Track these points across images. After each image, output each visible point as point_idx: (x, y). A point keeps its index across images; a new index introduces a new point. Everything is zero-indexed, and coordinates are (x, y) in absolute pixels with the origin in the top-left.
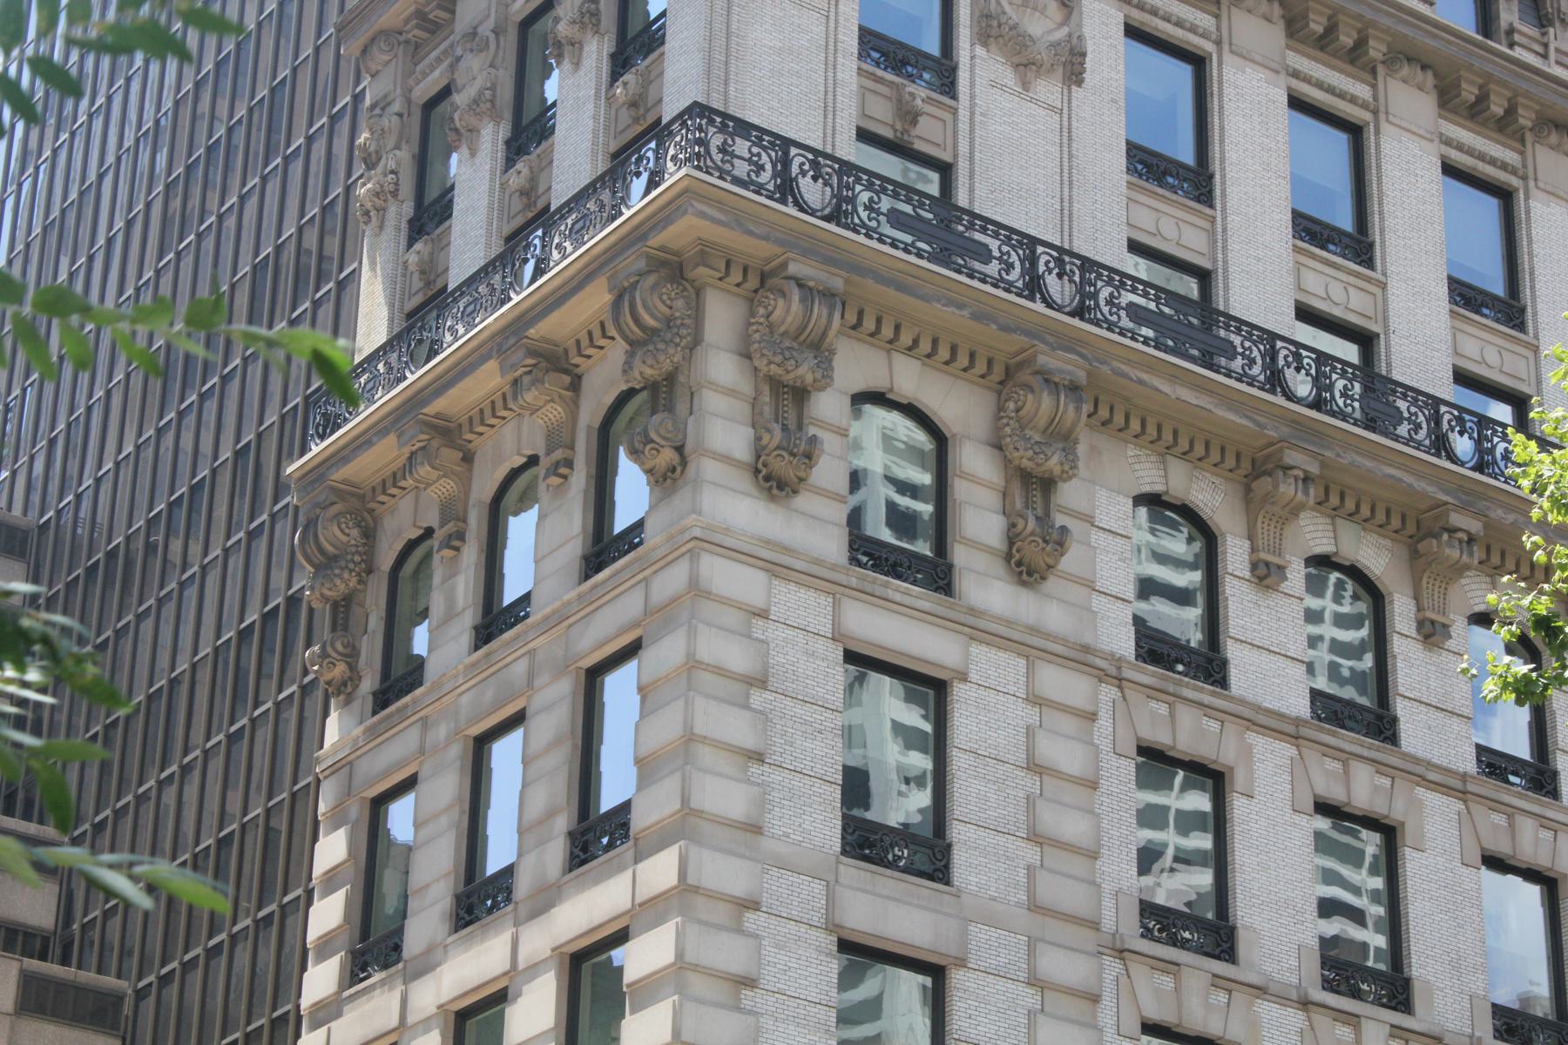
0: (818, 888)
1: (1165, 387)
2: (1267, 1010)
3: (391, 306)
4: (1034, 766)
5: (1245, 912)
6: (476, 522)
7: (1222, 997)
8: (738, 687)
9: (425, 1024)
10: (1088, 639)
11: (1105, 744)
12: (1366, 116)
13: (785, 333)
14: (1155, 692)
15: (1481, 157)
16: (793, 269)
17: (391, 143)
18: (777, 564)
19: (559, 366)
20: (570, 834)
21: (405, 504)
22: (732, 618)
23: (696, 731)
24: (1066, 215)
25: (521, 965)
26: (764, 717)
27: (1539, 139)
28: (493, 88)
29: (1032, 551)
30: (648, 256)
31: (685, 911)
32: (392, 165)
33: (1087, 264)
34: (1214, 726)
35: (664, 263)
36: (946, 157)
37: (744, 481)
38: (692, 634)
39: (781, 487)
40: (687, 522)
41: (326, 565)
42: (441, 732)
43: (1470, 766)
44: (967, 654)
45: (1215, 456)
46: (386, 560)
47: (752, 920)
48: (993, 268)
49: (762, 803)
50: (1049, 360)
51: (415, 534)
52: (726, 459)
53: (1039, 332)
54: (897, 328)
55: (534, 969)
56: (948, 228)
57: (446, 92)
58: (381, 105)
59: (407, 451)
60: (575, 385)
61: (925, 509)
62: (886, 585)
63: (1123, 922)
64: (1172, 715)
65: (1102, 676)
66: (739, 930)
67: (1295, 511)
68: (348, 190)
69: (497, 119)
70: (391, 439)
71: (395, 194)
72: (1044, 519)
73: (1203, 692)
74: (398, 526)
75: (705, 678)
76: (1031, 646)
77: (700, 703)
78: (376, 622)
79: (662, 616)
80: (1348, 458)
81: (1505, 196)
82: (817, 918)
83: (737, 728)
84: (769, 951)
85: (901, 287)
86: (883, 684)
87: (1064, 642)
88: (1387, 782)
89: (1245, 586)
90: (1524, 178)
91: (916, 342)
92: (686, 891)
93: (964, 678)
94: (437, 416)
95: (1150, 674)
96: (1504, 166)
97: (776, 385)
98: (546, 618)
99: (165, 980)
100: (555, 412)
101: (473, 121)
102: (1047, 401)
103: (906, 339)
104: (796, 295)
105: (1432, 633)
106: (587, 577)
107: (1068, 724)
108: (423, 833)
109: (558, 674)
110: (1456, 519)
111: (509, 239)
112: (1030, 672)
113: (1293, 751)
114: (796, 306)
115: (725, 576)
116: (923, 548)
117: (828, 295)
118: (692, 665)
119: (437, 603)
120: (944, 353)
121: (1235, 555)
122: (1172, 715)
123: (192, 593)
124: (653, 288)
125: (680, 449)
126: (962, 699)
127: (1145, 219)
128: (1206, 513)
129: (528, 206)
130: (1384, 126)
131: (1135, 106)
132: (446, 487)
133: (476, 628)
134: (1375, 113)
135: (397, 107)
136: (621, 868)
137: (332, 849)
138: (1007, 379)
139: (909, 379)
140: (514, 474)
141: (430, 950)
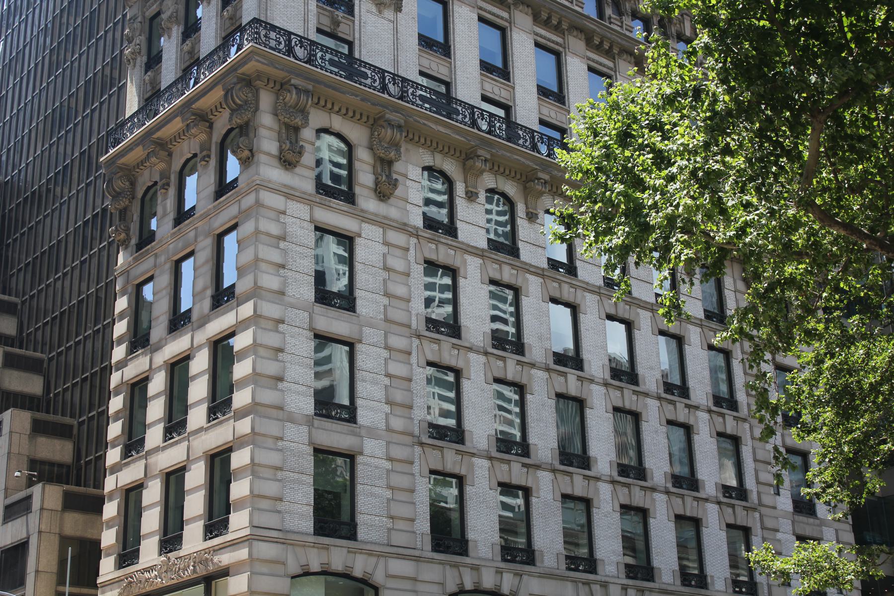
0: (306, 314)
1: (433, 126)
2: (472, 356)
3: (139, 96)
4: (386, 268)
5: (465, 320)
6: (174, 178)
7: (456, 352)
8: (274, 241)
9: (159, 369)
10: (405, 221)
11: (412, 260)
12: (507, 24)
13: (290, 107)
14: (430, 240)
15: (549, 40)
16: (293, 81)
17: (137, 34)
18: (289, 194)
19: (205, 119)
20: (213, 297)
21: (146, 173)
22: (272, 214)
23: (260, 256)
24: (396, 62)
25: (195, 346)
26: (285, 252)
27: (570, 34)
28: (177, 12)
29: (385, 188)
30: (238, 77)
31: (256, 324)
32: (138, 42)
33: (404, 80)
34: (453, 252)
35: (244, 80)
36: (351, 39)
37: (275, 162)
38: (257, 220)
39: (289, 165)
40: (255, 178)
41: (116, 196)
42: (162, 259)
43: (546, 266)
44: (361, 228)
45: (452, 152)
46: (140, 194)
47: (282, 327)
48: (369, 81)
49: (285, 283)
50: (390, 116)
51: (150, 184)
52: (269, 154)
53: (386, 105)
54: (333, 104)
55: (200, 347)
56: (352, 66)
57: (158, 14)
58: (134, 18)
59: (146, 152)
60: (211, 126)
61: (344, 173)
62: (330, 201)
63: (418, 324)
64: (437, 248)
65: (411, 235)
66: (277, 331)
67: (482, 172)
68: (122, 51)
69: (178, 24)
70: (140, 148)
71: (139, 53)
72: (389, 176)
73: (449, 240)
74: (145, 179)
75: (263, 237)
76: (384, 223)
77: (261, 247)
78: (136, 217)
79: (245, 214)
80: (501, 152)
81: (558, 55)
82: (306, 326)
83: (275, 256)
84: (288, 339)
85: (335, 89)
86: (330, 239)
87: (397, 222)
88: (515, 272)
89: (464, 201)
90: (565, 48)
91: (340, 109)
92: (257, 317)
93: (360, 236)
94: (158, 138)
95: (428, 233)
96: (557, 44)
97: (288, 126)
98: (202, 215)
99: (60, 354)
100: (203, 137)
101: (169, 25)
102: (389, 131)
103: (336, 108)
104: (294, 92)
105: (532, 217)
106: (217, 200)
107: (398, 252)
108: (156, 297)
109: (206, 237)
110: (541, 175)
111: (184, 70)
112: (384, 232)
113: (481, 261)
114: (294, 96)
115: (268, 198)
116: (344, 188)
117: (307, 92)
118: (257, 232)
119: (160, 210)
120: (351, 114)
121: (460, 189)
122: (437, 248)
123: (65, 207)
124: (240, 89)
125: (251, 151)
126: (359, 243)
127: (426, 63)
128: (449, 173)
129: (191, 58)
130: (513, 28)
131: (421, 19)
132: (162, 166)
133: (175, 219)
134: (510, 23)
135: (139, 19)
136: (232, 309)
137: (122, 304)
138: (374, 123)
139: (337, 123)
140: (188, 160)
141: (160, 340)
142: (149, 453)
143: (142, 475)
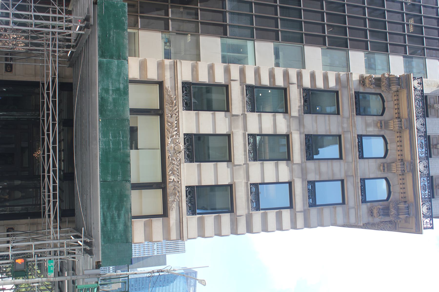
9: (289, 126)
143: (234, 113)
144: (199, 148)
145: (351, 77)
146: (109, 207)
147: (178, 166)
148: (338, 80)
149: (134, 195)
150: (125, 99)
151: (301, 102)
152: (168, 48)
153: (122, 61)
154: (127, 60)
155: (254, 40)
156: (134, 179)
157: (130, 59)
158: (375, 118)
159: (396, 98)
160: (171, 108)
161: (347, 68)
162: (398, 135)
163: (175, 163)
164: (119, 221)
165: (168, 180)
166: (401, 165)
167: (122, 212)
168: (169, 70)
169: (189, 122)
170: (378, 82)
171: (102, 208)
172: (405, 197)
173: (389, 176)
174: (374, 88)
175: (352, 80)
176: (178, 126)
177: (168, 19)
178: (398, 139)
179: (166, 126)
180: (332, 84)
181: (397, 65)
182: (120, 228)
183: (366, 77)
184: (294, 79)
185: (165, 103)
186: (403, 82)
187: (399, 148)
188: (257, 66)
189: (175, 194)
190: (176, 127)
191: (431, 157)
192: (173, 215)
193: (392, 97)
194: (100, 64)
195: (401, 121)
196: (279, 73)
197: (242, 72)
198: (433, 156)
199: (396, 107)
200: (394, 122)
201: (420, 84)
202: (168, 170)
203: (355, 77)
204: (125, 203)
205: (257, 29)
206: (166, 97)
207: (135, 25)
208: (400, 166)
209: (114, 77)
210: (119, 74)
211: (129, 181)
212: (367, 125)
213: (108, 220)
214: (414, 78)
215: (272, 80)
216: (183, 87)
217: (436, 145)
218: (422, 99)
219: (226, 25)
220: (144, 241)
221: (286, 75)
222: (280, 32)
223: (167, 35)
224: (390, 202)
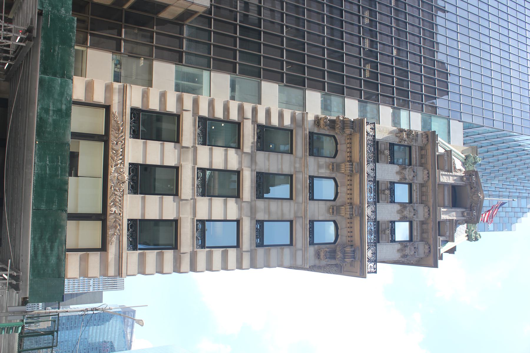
9: (240, 163)
141: (256, 163)
142: (195, 149)
143: (184, 145)
144: (144, 179)
145: (307, 117)
146: (41, 239)
147: (120, 197)
148: (293, 118)
149: (71, 226)
150: (66, 121)
151: (254, 139)
152: (118, 70)
153: (66, 80)
154: (72, 80)
155: (210, 71)
156: (71, 208)
157: (75, 78)
158: (327, 159)
159: (349, 141)
160: (117, 135)
161: (303, 107)
162: (349, 178)
163: (118, 193)
164: (51, 253)
165: (109, 212)
166: (350, 208)
167: (56, 244)
168: (117, 94)
169: (137, 151)
170: (332, 124)
171: (33, 239)
172: (352, 241)
173: (338, 219)
174: (328, 129)
175: (307, 120)
176: (123, 154)
177: (121, 40)
178: (349, 183)
179: (111, 153)
180: (287, 122)
181: (352, 109)
182: (52, 261)
183: (321, 118)
184: (249, 114)
185: (111, 129)
186: (357, 126)
187: (349, 192)
188: (212, 97)
189: (116, 227)
190: (121, 155)
191: (378, 202)
192: (112, 249)
193: (345, 140)
194: (41, 81)
195: (352, 165)
196: (234, 106)
197: (196, 103)
198: (380, 201)
199: (348, 150)
200: (345, 165)
201: (373, 129)
202: (109, 201)
203: (311, 117)
204: (59, 235)
205: (214, 59)
206: (112, 122)
207: (84, 43)
208: (348, 210)
209: (56, 96)
210: (62, 94)
211: (66, 211)
212: (319, 167)
213: (40, 252)
214: (368, 123)
215: (226, 113)
216: (131, 113)
217: (384, 191)
218: (374, 145)
219: (182, 52)
220: (78, 277)
221: (241, 109)
222: (237, 65)
223: (118, 57)
224: (337, 245)
